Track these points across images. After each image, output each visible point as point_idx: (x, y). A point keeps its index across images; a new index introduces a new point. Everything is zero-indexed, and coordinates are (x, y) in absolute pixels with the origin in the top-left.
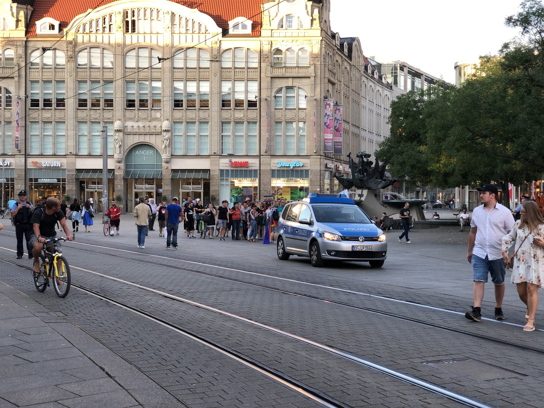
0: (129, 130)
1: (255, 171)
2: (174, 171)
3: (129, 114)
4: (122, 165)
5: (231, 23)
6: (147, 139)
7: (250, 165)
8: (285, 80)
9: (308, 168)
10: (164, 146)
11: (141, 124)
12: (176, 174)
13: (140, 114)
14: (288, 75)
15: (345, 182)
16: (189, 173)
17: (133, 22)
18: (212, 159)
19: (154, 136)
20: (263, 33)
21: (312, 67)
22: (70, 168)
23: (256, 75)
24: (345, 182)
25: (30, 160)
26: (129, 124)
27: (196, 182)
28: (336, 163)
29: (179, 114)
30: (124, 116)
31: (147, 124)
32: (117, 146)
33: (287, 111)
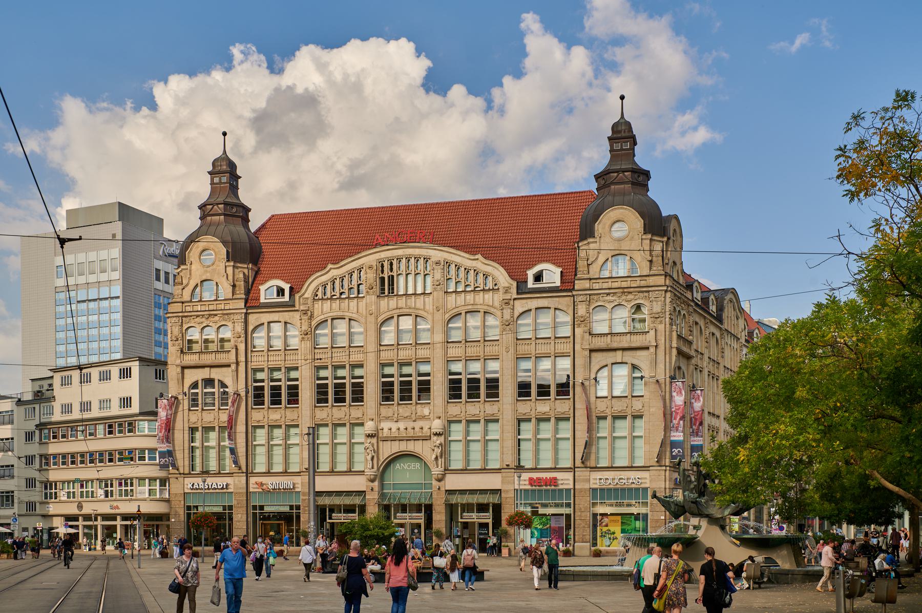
0: (386, 433)
1: (568, 490)
2: (450, 492)
3: (385, 411)
5: (531, 273)
6: (411, 447)
8: (611, 354)
9: (647, 486)
10: (434, 456)
11: (402, 425)
12: (450, 497)
13: (401, 410)
14: (615, 345)
15: (673, 506)
16: (471, 496)
17: (391, 278)
19: (421, 442)
20: (578, 285)
21: (652, 333)
23: (568, 348)
24: (673, 506)
26: (385, 425)
27: (482, 508)
29: (525, 407)
30: (379, 414)
31: (410, 424)
32: (369, 457)
33: (614, 400)
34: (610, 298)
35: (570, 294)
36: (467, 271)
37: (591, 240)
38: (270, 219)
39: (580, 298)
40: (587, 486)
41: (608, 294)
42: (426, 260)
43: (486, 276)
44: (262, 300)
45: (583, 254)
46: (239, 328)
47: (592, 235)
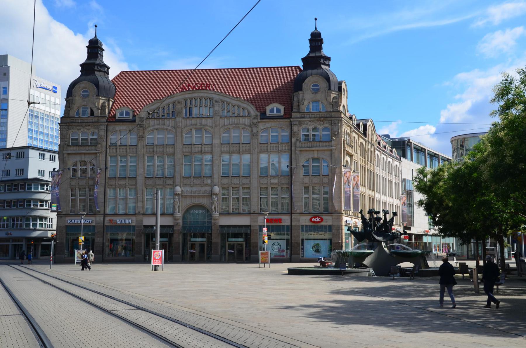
1: (288, 226)
2: (222, 226)
4: (181, 221)
5: (268, 109)
7: (283, 221)
9: (331, 224)
11: (194, 189)
18: (252, 217)
25: (107, 219)
28: (354, 220)
34: (309, 123)
36: (233, 106)
37: (300, 92)
38: (121, 73)
39: (295, 123)
40: (298, 224)
41: (309, 121)
42: (211, 99)
43: (244, 109)
44: (117, 118)
45: (295, 99)
46: (103, 133)
47: (301, 89)
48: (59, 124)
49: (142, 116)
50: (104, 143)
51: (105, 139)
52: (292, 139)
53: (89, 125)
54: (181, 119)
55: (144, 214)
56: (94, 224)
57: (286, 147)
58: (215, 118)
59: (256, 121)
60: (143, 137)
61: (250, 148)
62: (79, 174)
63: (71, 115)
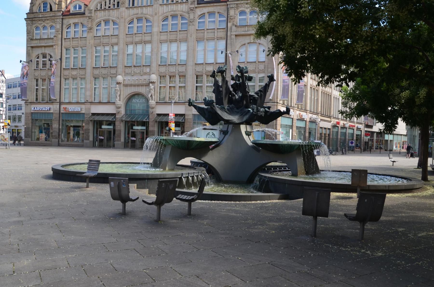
6: (142, 90)
8: (248, 37)
10: (150, 95)
11: (135, 78)
22: (88, 112)
25: (62, 106)
34: (246, 6)
35: (225, 4)
39: (231, 6)
44: (71, 12)
46: (59, 26)
48: (25, 19)
49: (91, 9)
50: (60, 36)
51: (60, 33)
52: (228, 24)
53: (48, 20)
54: (124, 9)
55: (91, 103)
56: (51, 111)
57: (222, 34)
58: (155, 6)
59: (193, 6)
60: (91, 29)
61: (187, 35)
62: (41, 66)
63: (34, 11)
